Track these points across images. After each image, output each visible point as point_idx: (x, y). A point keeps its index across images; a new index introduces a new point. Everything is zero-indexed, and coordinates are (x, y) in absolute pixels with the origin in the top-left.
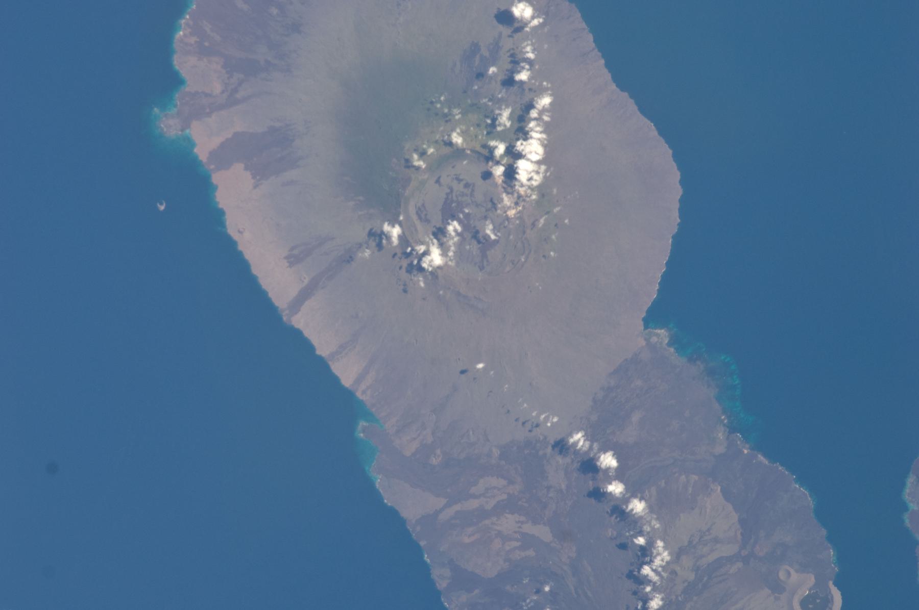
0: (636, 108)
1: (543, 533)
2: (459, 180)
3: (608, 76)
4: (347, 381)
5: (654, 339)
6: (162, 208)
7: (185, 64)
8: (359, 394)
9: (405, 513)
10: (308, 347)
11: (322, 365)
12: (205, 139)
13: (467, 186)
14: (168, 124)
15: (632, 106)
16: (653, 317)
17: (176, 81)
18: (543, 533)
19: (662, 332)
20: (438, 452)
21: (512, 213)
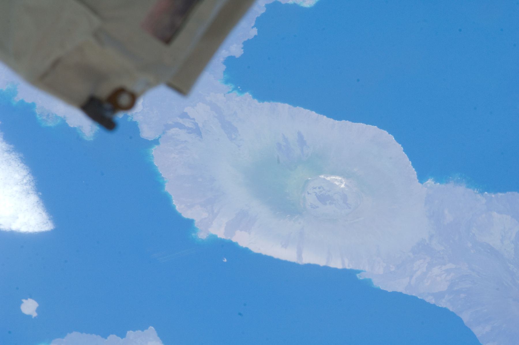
0: (350, 123)
1: (450, 266)
2: (315, 188)
3: (332, 120)
4: (340, 266)
5: (429, 185)
6: (225, 260)
7: (187, 214)
8: (347, 268)
9: (399, 290)
10: (316, 267)
11: (326, 269)
12: (219, 230)
13: (319, 188)
14: (202, 235)
15: (349, 123)
16: (422, 178)
17: (190, 222)
18: (450, 266)
19: (428, 181)
20: (391, 266)
21: (343, 186)
